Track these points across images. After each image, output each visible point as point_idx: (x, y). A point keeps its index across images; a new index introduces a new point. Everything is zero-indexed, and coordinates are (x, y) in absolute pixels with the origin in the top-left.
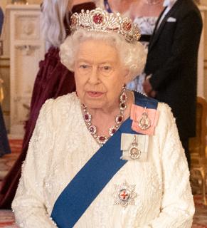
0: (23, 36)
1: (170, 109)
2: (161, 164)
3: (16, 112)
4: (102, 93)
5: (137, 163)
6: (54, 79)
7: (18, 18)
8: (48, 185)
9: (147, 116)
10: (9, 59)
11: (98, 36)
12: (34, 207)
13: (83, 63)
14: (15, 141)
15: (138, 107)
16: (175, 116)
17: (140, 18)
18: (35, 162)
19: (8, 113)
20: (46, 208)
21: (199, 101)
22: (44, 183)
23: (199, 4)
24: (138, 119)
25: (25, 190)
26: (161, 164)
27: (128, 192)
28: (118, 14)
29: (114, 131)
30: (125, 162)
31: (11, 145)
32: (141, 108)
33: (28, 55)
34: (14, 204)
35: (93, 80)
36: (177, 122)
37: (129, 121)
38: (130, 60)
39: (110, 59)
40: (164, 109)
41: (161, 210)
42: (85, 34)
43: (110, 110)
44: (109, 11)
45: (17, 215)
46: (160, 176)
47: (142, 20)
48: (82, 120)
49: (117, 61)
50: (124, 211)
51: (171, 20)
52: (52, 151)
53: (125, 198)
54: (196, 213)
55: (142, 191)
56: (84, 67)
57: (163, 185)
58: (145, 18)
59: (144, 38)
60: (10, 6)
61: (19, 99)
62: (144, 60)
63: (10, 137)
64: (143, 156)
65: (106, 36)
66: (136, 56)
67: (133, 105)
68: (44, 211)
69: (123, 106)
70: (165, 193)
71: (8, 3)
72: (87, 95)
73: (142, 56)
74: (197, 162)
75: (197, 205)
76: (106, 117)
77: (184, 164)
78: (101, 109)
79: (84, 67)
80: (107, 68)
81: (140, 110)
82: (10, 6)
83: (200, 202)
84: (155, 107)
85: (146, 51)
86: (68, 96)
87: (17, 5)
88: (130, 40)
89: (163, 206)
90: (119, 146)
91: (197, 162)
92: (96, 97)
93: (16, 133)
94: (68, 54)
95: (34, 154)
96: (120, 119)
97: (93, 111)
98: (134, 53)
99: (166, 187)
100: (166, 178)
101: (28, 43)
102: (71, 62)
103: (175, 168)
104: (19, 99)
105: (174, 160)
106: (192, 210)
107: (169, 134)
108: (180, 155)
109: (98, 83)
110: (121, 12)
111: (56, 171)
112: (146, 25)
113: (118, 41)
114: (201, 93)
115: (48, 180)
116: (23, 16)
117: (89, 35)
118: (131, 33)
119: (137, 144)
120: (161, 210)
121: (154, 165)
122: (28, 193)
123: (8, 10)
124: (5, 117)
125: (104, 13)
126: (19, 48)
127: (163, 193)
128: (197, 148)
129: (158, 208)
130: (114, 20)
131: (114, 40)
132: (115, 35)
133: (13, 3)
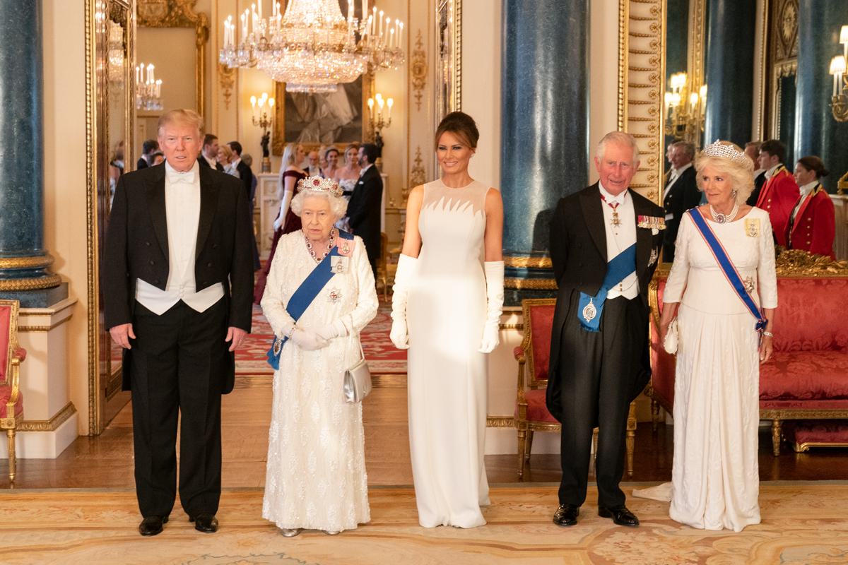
0: (269, 193)
1: (362, 240)
2: (357, 275)
3: (265, 243)
4: (319, 230)
5: (342, 275)
6: (293, 223)
7: (266, 182)
8: (284, 290)
9: (347, 244)
10: (260, 209)
11: (317, 193)
12: (275, 304)
13: (308, 211)
14: (263, 261)
15: (342, 239)
16: (365, 244)
17: (345, 180)
18: (275, 275)
19: (260, 243)
20: (282, 304)
21: (382, 235)
22: (282, 288)
23: (382, 172)
24: (342, 247)
25: (269, 293)
26: (357, 275)
27: (336, 293)
28: (329, 179)
29: (326, 254)
30: (334, 274)
31: (262, 264)
32: (344, 239)
33: (272, 205)
34: (262, 303)
35: (314, 222)
36: (366, 248)
37: (336, 248)
38: (337, 209)
39: (325, 209)
40: (358, 240)
41: (357, 305)
42: (309, 193)
43: (323, 240)
44: (324, 178)
45: (264, 310)
46: (356, 283)
47: (346, 182)
48: (306, 248)
49: (329, 210)
50: (334, 306)
51: (361, 183)
52: (287, 268)
53: (335, 297)
54: (380, 306)
55: (345, 294)
56: (308, 213)
57: (358, 289)
58: (349, 180)
59: (346, 193)
60: (260, 174)
61: (266, 234)
62: (346, 208)
63: (261, 258)
64: (345, 270)
65: (322, 194)
66: (341, 206)
67: (339, 237)
68: (281, 306)
69: (332, 238)
70: (360, 293)
71: (259, 172)
72: (311, 231)
73: (344, 206)
74: (381, 274)
75: (380, 302)
76: (321, 245)
77: (372, 275)
78: (318, 240)
79: (308, 213)
80: (322, 214)
81: (343, 240)
82: (260, 174)
83: (382, 299)
84: (353, 239)
85: (348, 202)
86: (296, 232)
87: (264, 174)
88: (337, 195)
89: (359, 301)
90: (330, 264)
91: (381, 274)
92: (316, 232)
93: (264, 256)
94: (297, 205)
95: (275, 270)
96: (330, 247)
97: (313, 242)
98: (340, 204)
99: (360, 290)
100: (360, 284)
101: (272, 198)
102: (299, 211)
103: (366, 278)
104: (266, 234)
105: (365, 273)
106: (377, 305)
107: (362, 255)
108: (369, 269)
109: (317, 224)
110: (331, 177)
111: (290, 281)
112: (350, 185)
113: (330, 196)
114: (383, 230)
115: (284, 286)
116: (269, 181)
117: (311, 193)
118: (337, 191)
119: (341, 263)
120: (357, 305)
121: (352, 276)
122: (271, 294)
123: (259, 177)
124: (258, 246)
125: (320, 179)
126: (266, 202)
127: (358, 294)
128: (381, 265)
129: (355, 304)
130: (327, 183)
131: (327, 196)
132: (328, 193)
133: (263, 172)
